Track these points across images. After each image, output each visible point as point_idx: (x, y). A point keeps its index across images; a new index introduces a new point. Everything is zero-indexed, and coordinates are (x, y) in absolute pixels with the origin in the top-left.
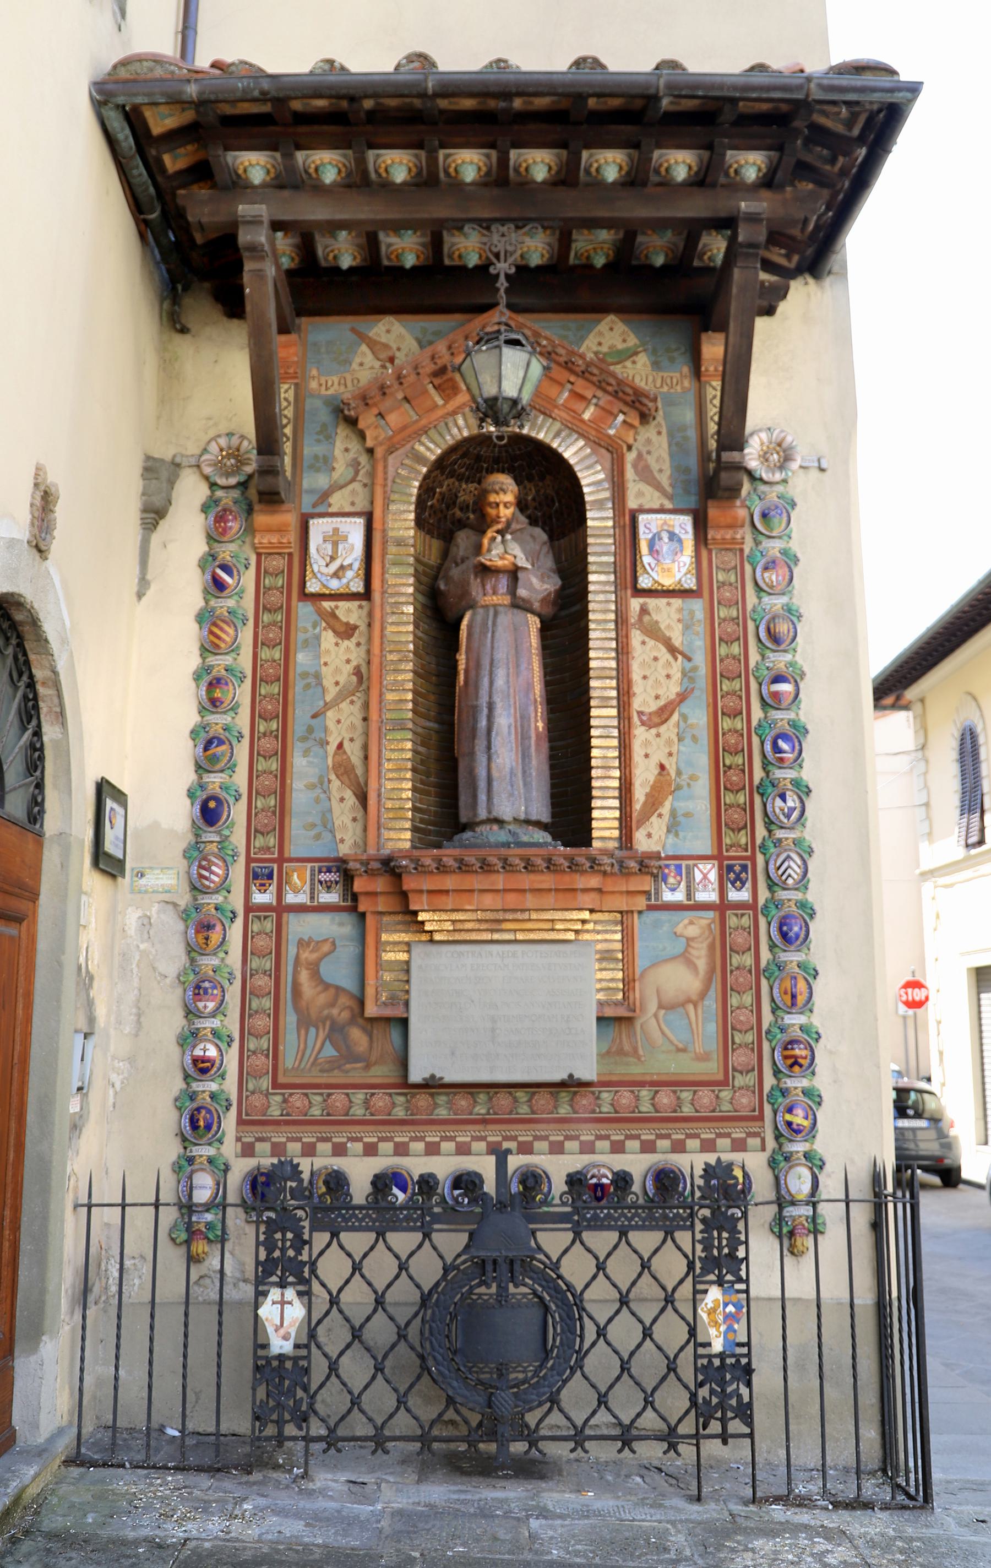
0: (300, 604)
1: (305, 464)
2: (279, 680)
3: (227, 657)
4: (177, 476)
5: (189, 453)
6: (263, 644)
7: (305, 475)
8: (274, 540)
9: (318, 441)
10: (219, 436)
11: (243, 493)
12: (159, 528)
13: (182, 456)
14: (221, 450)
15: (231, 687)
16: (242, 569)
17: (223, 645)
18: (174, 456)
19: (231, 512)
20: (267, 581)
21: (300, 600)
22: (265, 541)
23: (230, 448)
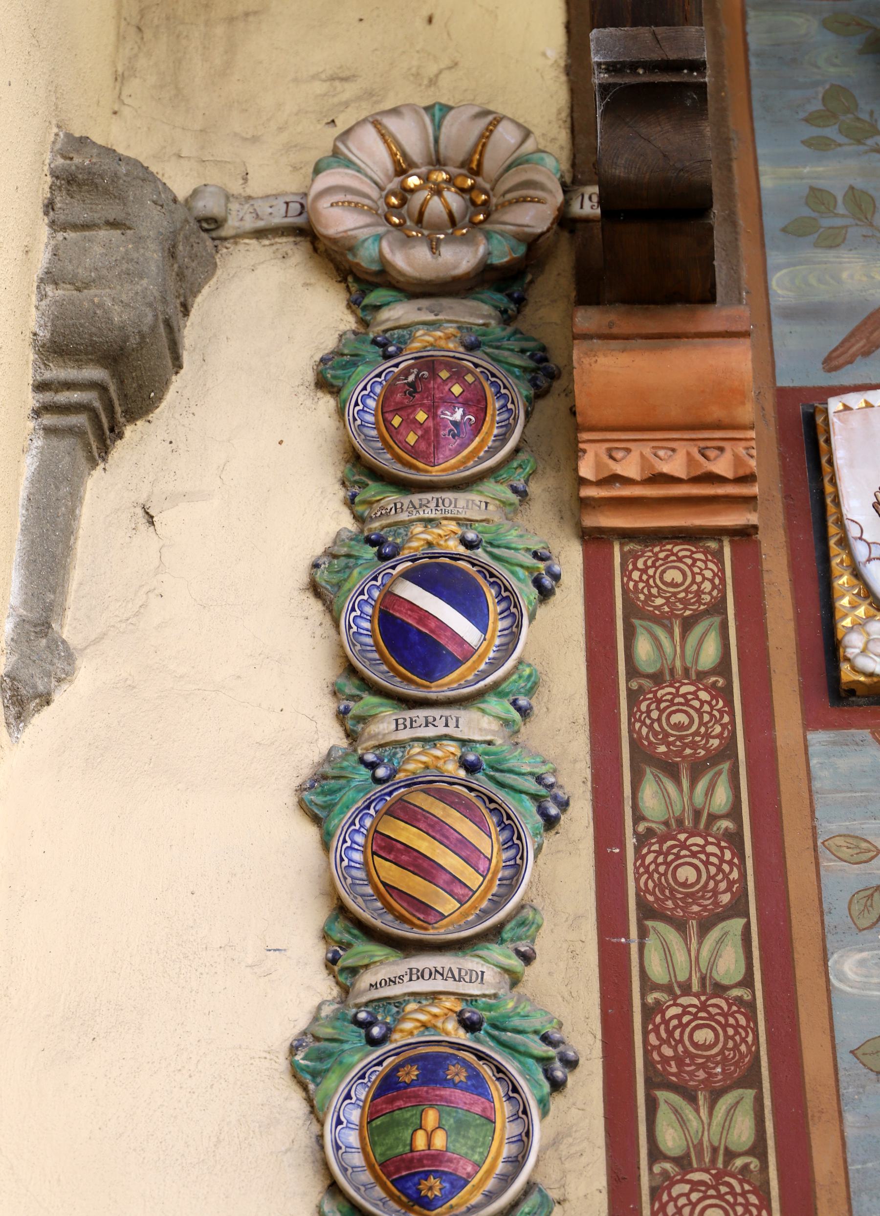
0: (818, 738)
1: (772, 222)
2: (751, 1079)
3: (469, 963)
4: (210, 268)
5: (255, 188)
6: (647, 912)
7: (774, 258)
8: (675, 466)
9: (820, 145)
10: (395, 111)
11: (506, 318)
12: (120, 451)
13: (228, 197)
14: (401, 171)
15: (503, 1109)
16: (526, 594)
17: (447, 905)
18: (195, 193)
19: (458, 375)
20: (644, 648)
21: (811, 722)
22: (630, 468)
23: (438, 162)
